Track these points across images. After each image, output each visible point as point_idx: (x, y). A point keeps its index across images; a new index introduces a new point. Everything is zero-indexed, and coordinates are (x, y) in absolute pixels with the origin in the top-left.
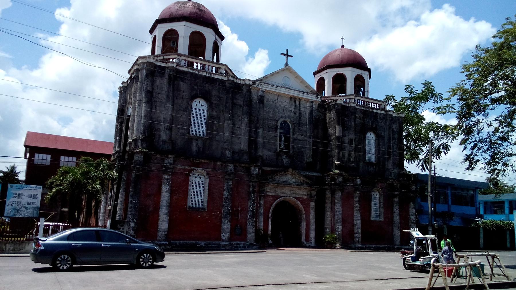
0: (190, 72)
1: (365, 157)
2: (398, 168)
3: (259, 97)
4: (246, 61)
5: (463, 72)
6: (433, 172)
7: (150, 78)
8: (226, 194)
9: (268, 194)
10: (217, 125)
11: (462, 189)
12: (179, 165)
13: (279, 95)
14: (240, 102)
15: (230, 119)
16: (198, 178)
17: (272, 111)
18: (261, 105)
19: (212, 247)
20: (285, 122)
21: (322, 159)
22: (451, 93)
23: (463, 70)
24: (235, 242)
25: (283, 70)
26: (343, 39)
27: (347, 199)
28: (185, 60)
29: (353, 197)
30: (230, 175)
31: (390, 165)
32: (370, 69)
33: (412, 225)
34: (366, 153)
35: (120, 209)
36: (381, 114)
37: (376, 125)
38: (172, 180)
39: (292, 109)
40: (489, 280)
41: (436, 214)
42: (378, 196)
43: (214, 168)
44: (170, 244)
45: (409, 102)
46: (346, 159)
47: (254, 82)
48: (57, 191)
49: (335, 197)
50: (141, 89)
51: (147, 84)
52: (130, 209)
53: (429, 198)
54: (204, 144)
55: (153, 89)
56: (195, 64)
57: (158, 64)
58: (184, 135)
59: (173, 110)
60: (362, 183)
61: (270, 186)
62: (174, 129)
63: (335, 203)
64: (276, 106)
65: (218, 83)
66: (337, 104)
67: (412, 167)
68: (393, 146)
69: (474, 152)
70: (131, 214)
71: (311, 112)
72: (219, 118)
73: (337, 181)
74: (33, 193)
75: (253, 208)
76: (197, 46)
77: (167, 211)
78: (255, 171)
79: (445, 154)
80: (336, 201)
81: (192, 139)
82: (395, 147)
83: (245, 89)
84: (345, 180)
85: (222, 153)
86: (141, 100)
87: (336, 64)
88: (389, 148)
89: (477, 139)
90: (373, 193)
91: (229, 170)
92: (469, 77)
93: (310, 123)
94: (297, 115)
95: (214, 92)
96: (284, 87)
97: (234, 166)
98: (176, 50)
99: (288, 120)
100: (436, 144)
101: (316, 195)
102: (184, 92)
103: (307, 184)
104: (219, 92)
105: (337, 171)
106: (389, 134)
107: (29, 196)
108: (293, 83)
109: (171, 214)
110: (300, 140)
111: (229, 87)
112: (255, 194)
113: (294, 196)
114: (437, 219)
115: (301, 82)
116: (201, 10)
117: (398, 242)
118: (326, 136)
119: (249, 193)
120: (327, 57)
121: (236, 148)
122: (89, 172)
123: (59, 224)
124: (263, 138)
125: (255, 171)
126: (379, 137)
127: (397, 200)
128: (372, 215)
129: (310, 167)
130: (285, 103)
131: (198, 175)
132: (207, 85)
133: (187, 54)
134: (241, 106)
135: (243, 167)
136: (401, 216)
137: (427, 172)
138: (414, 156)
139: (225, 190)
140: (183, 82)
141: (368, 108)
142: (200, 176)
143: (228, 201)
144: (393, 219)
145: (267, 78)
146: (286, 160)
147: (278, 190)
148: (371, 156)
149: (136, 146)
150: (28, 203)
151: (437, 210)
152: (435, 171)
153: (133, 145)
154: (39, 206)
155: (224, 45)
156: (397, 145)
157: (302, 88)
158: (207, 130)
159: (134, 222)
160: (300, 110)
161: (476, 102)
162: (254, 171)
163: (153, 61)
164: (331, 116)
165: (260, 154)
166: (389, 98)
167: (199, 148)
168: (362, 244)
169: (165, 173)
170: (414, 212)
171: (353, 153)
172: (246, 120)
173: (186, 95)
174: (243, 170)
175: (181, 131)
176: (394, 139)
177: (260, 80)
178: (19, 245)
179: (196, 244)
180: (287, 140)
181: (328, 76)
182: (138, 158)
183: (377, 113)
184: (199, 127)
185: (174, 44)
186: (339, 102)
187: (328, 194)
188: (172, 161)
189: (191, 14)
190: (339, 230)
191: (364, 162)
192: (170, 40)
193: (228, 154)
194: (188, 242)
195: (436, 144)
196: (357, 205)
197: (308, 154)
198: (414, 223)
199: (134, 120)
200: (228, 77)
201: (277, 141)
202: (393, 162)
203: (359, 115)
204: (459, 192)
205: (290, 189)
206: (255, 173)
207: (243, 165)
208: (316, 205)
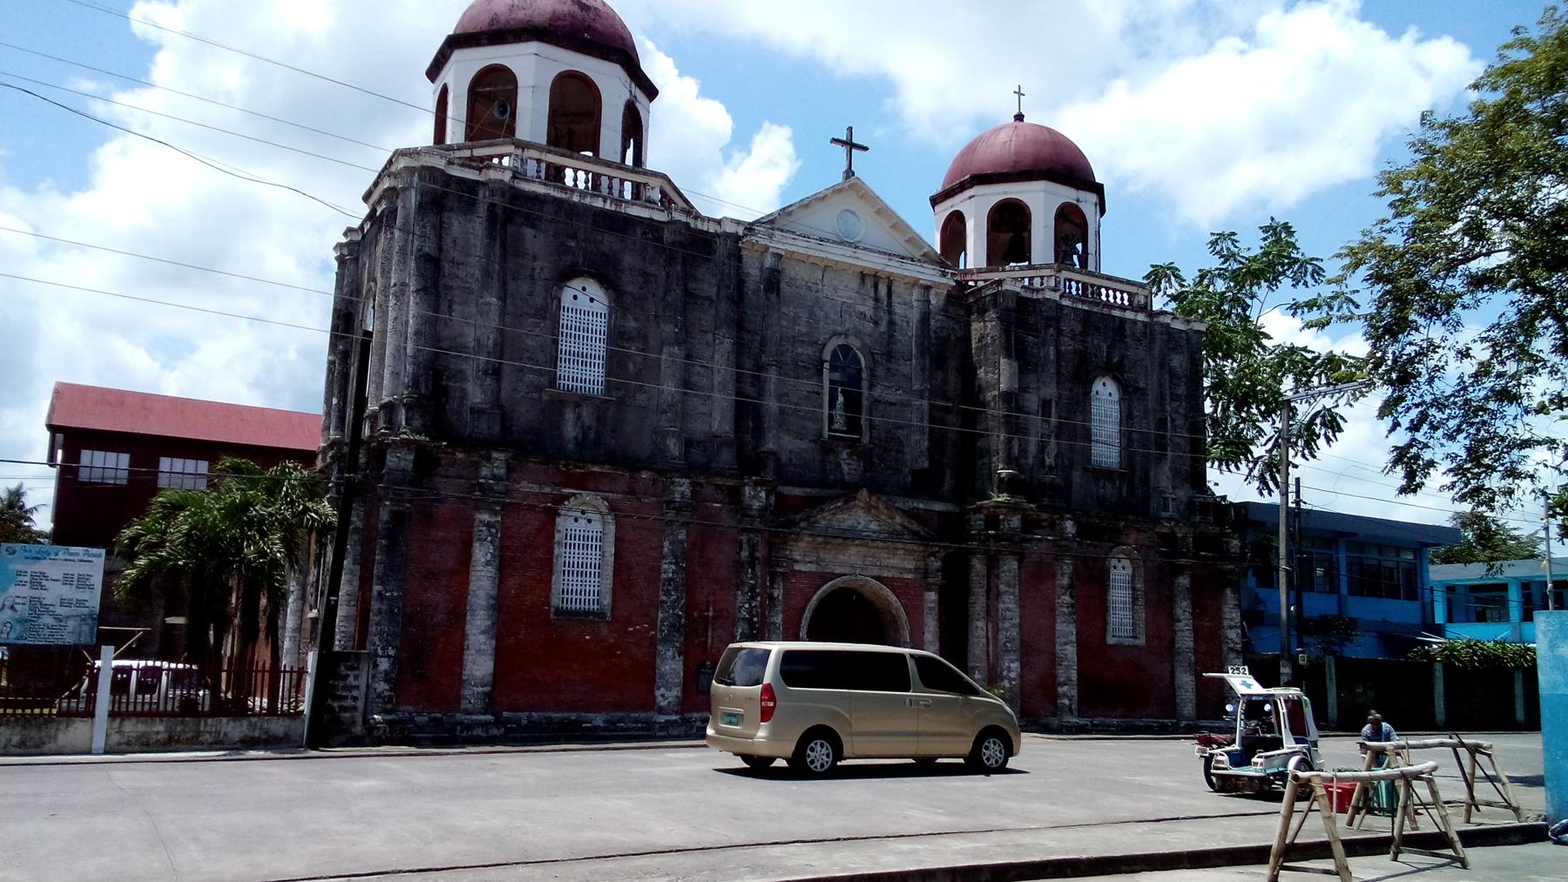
0: (555, 199)
1: (1087, 453)
2: (1187, 486)
3: (766, 275)
4: (724, 164)
5: (1381, 194)
6: (1292, 497)
7: (431, 217)
8: (668, 569)
9: (797, 567)
10: (640, 360)
11: (1381, 548)
12: (524, 483)
15: (678, 342)
16: (582, 522)
17: (804, 315)
18: (773, 298)
19: (628, 729)
20: (846, 349)
21: (958, 463)
22: (1347, 261)
23: (1381, 189)
24: (696, 715)
25: (837, 190)
26: (1020, 94)
27: (1036, 578)
28: (539, 161)
29: (1054, 576)
30: (679, 511)
31: (1163, 477)
32: (1101, 186)
33: (1232, 656)
34: (1090, 441)
35: (347, 617)
36: (1135, 322)
37: (1123, 357)
38: (504, 528)
39: (868, 308)
40: (1463, 819)
41: (1302, 626)
42: (1129, 571)
43: (631, 492)
44: (499, 722)
45: (1220, 286)
46: (1030, 460)
47: (750, 228)
48: (153, 568)
49: (997, 577)
50: (403, 251)
51: (423, 236)
52: (377, 619)
53: (1282, 575)
54: (600, 419)
55: (440, 250)
56: (569, 173)
57: (456, 172)
58: (539, 389)
59: (503, 313)
60: (1082, 531)
61: (802, 544)
62: (506, 370)
63: (998, 594)
64: (817, 301)
65: (639, 231)
66: (1005, 294)
67: (1231, 484)
68: (1173, 420)
69: (1419, 436)
70: (381, 633)
71: (925, 319)
72: (645, 338)
73: (1005, 527)
74: (76, 569)
75: (749, 611)
76: (574, 118)
77: (488, 623)
78: (755, 497)
79: (1328, 440)
80: (1002, 587)
81: (561, 402)
82: (1180, 422)
83: (721, 249)
84: (1029, 525)
85: (655, 443)
86: (404, 284)
87: (999, 170)
88: (1162, 424)
89: (1428, 399)
90: (1114, 562)
91: (677, 497)
92: (1401, 208)
93: (922, 354)
94: (882, 328)
95: (628, 260)
96: (842, 243)
97: (694, 484)
98: (511, 130)
99: (854, 342)
100: (1304, 410)
101: (943, 569)
102: (535, 258)
103: (915, 535)
104: (644, 259)
105: (1003, 498)
106: (1161, 385)
107: (67, 580)
108: (868, 229)
110: (892, 404)
111: (673, 243)
112: (758, 567)
113: (876, 572)
114: (1306, 639)
115: (893, 227)
117: (1188, 709)
118: (971, 390)
119: (739, 566)
120: (971, 149)
121: (698, 428)
122: (247, 504)
123: (158, 664)
124: (780, 398)
125: (755, 497)
126: (1129, 392)
127: (1184, 581)
128: (1110, 627)
129: (923, 484)
130: (846, 292)
131: (583, 512)
132: (607, 238)
133: (543, 140)
134: (712, 301)
135: (718, 487)
136: (1196, 630)
137: (1276, 498)
138: (1236, 450)
139: (664, 557)
140: (533, 227)
141: (1097, 304)
142: (589, 516)
143: (676, 589)
144: (1173, 642)
145: (790, 214)
146: (849, 466)
147: (826, 555)
148: (1107, 450)
149: (391, 424)
150: (62, 602)
151: (1306, 613)
152: (1298, 492)
153: (381, 424)
154: (97, 610)
155: (656, 116)
156: (1186, 417)
157: (896, 244)
158: (608, 374)
159: (389, 656)
160: (890, 312)
161: (1422, 287)
162: (755, 497)
163: (440, 164)
164: (985, 328)
165: (771, 446)
166: (1158, 275)
167: (585, 430)
168: (1081, 714)
169: (480, 506)
170: (1238, 619)
171: (1053, 440)
172: (728, 343)
173: (543, 266)
174: (719, 497)
175: (530, 377)
176: (1175, 397)
177: (770, 222)
178: (40, 729)
179: (579, 722)
180: (853, 404)
181: (976, 207)
182: (399, 461)
183: (1123, 321)
184: (583, 366)
185: (503, 113)
186: (1005, 287)
187: (978, 565)
188: (502, 471)
189: (555, 17)
190: (1013, 675)
191: (1085, 470)
192: (492, 98)
193: (673, 447)
194: (554, 715)
195: (1304, 410)
196: (1067, 598)
197: (916, 445)
198: (1237, 652)
199: (383, 346)
200: (669, 210)
201: (821, 406)
202: (1175, 472)
203: (1070, 326)
204: (1372, 557)
205: (864, 548)
206: (756, 504)
207: (719, 481)
208: (942, 601)
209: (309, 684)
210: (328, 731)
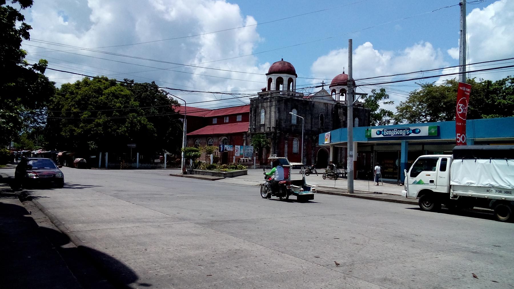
13: (320, 102)
14: (308, 109)
39: (325, 108)
45: (373, 98)
130: (322, 106)
173: (290, 108)
182: (278, 135)
189: (288, 69)
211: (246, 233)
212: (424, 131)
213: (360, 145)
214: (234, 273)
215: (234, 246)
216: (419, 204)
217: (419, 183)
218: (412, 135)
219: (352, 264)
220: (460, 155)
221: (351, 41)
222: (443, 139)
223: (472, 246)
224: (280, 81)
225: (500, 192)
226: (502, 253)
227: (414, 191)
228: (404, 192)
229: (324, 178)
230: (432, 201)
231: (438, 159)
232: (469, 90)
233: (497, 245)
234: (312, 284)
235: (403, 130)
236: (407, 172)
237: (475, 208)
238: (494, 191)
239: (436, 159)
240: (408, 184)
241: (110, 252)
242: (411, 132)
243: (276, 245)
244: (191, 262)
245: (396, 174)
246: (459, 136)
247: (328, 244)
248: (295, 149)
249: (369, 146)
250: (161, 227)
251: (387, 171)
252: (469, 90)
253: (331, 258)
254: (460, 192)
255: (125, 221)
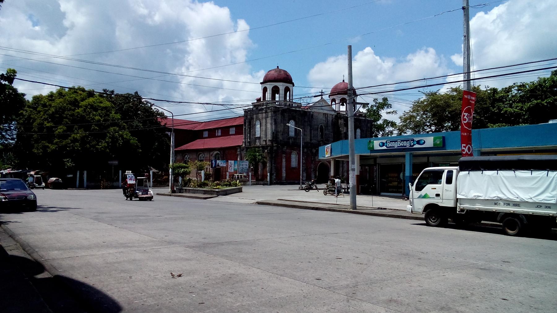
13: (319, 113)
14: (306, 120)
39: (324, 119)
45: (375, 108)
71: (332, 121)
81: (290, 138)
109: (286, 170)
116: (288, 75)
130: (321, 117)
173: (287, 119)
182: (275, 148)
189: (284, 78)
209: (268, 177)
210: (271, 183)
211: (241, 256)
212: (429, 141)
213: (362, 158)
214: (229, 300)
215: (229, 270)
216: (425, 219)
217: (425, 197)
218: (417, 146)
219: (356, 286)
220: (467, 166)
221: (350, 47)
222: (449, 150)
223: (480, 263)
224: (275, 90)
225: (509, 204)
226: (512, 268)
227: (420, 205)
228: (409, 207)
229: (325, 194)
230: (440, 216)
231: (444, 171)
232: (473, 98)
233: (506, 260)
234: (313, 308)
235: (407, 141)
236: (412, 185)
237: (482, 222)
238: (502, 203)
239: (442, 172)
240: (413, 198)
241: (90, 281)
242: (415, 143)
243: (274, 268)
244: (182, 290)
245: (401, 188)
246: (464, 147)
247: (330, 264)
248: (294, 163)
249: (371, 159)
250: (148, 252)
251: (391, 184)
252: (473, 98)
253: (334, 279)
254: (467, 206)
255: (109, 246)
